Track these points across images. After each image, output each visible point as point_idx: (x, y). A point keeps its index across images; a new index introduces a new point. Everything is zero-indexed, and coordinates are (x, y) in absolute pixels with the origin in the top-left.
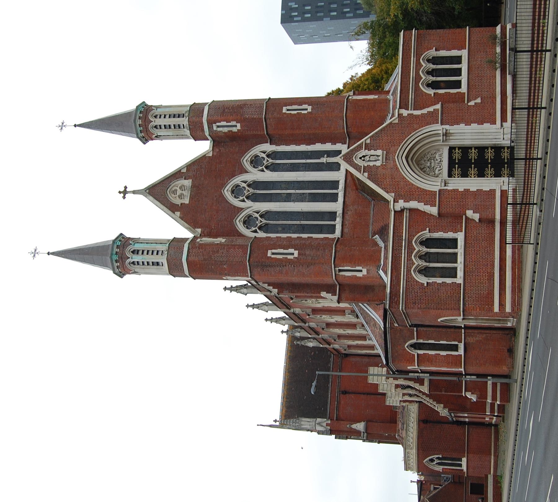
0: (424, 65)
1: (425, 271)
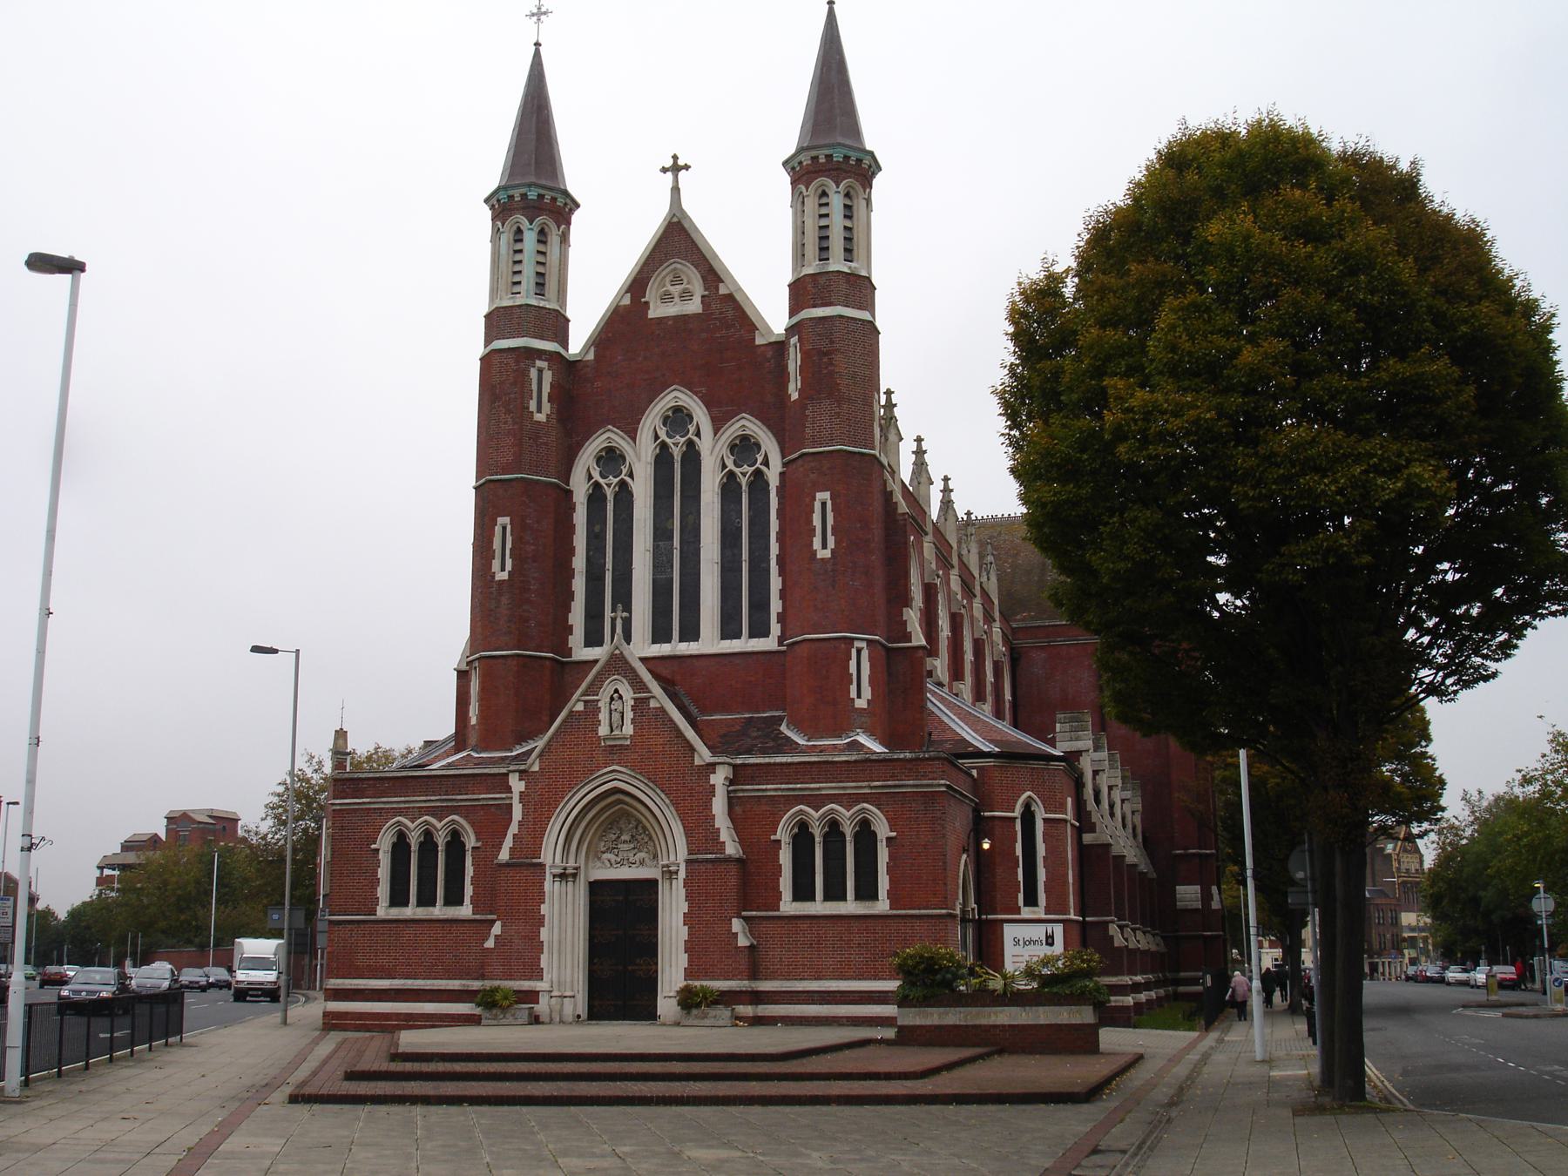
0: (848, 814)
1: (400, 847)
